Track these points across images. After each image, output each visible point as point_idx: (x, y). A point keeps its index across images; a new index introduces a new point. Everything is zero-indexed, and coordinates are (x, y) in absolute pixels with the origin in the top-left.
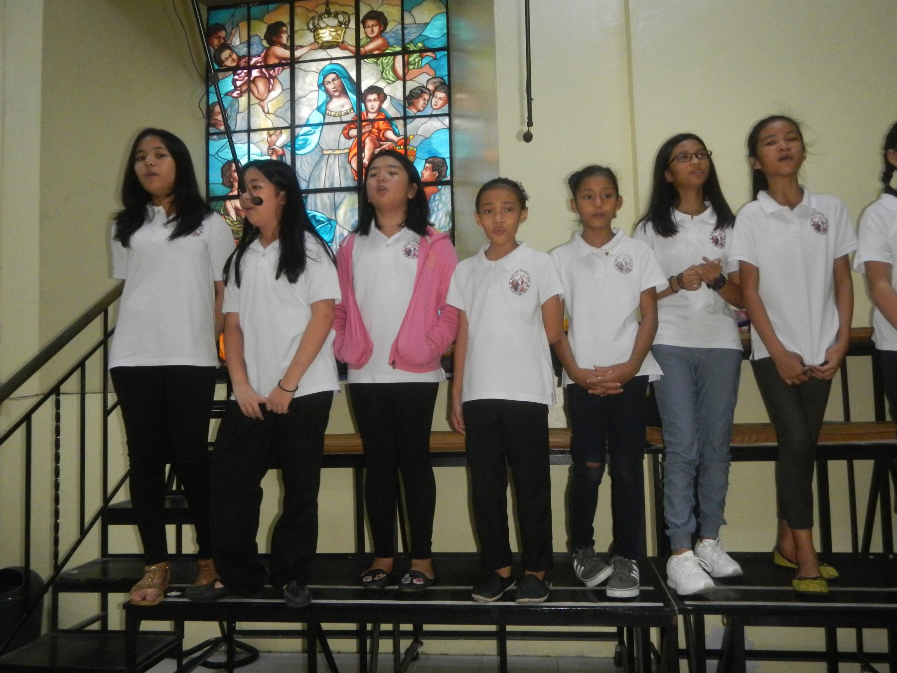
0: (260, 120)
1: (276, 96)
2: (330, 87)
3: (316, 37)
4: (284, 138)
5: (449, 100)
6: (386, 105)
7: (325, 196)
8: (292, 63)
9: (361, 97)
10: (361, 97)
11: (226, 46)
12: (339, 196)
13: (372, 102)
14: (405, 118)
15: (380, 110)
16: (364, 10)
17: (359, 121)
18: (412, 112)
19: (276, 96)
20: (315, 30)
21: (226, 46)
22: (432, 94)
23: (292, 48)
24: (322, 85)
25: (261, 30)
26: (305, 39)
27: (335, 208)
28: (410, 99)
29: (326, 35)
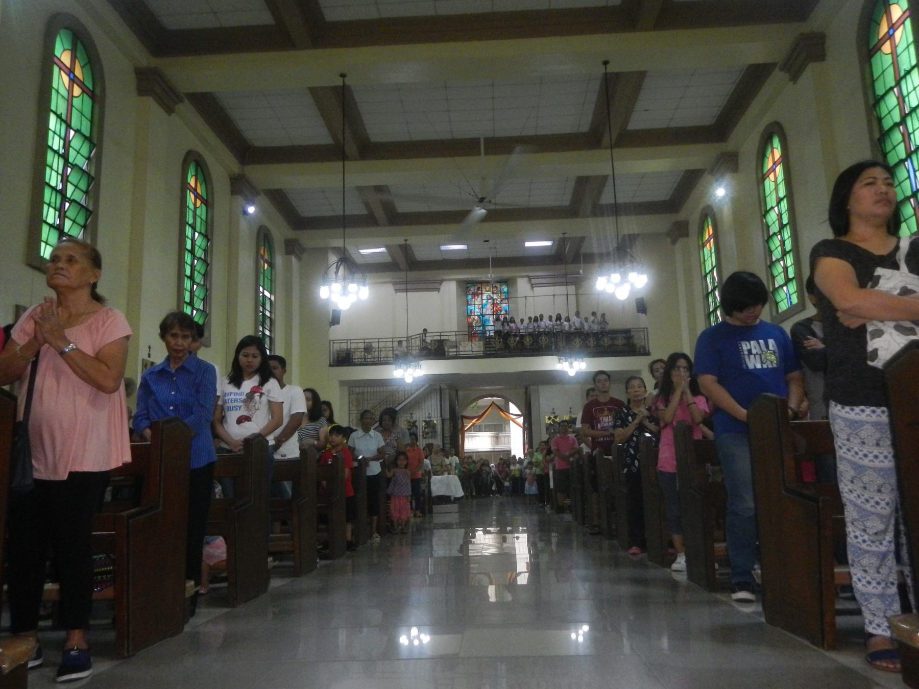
0: (476, 303)
1: (479, 299)
4: (481, 306)
5: (508, 301)
8: (482, 294)
10: (494, 300)
11: (470, 290)
14: (501, 304)
16: (494, 286)
19: (479, 299)
20: (486, 288)
21: (470, 290)
23: (482, 291)
24: (487, 298)
25: (476, 288)
26: (484, 290)
27: (490, 318)
28: (501, 301)
29: (487, 290)
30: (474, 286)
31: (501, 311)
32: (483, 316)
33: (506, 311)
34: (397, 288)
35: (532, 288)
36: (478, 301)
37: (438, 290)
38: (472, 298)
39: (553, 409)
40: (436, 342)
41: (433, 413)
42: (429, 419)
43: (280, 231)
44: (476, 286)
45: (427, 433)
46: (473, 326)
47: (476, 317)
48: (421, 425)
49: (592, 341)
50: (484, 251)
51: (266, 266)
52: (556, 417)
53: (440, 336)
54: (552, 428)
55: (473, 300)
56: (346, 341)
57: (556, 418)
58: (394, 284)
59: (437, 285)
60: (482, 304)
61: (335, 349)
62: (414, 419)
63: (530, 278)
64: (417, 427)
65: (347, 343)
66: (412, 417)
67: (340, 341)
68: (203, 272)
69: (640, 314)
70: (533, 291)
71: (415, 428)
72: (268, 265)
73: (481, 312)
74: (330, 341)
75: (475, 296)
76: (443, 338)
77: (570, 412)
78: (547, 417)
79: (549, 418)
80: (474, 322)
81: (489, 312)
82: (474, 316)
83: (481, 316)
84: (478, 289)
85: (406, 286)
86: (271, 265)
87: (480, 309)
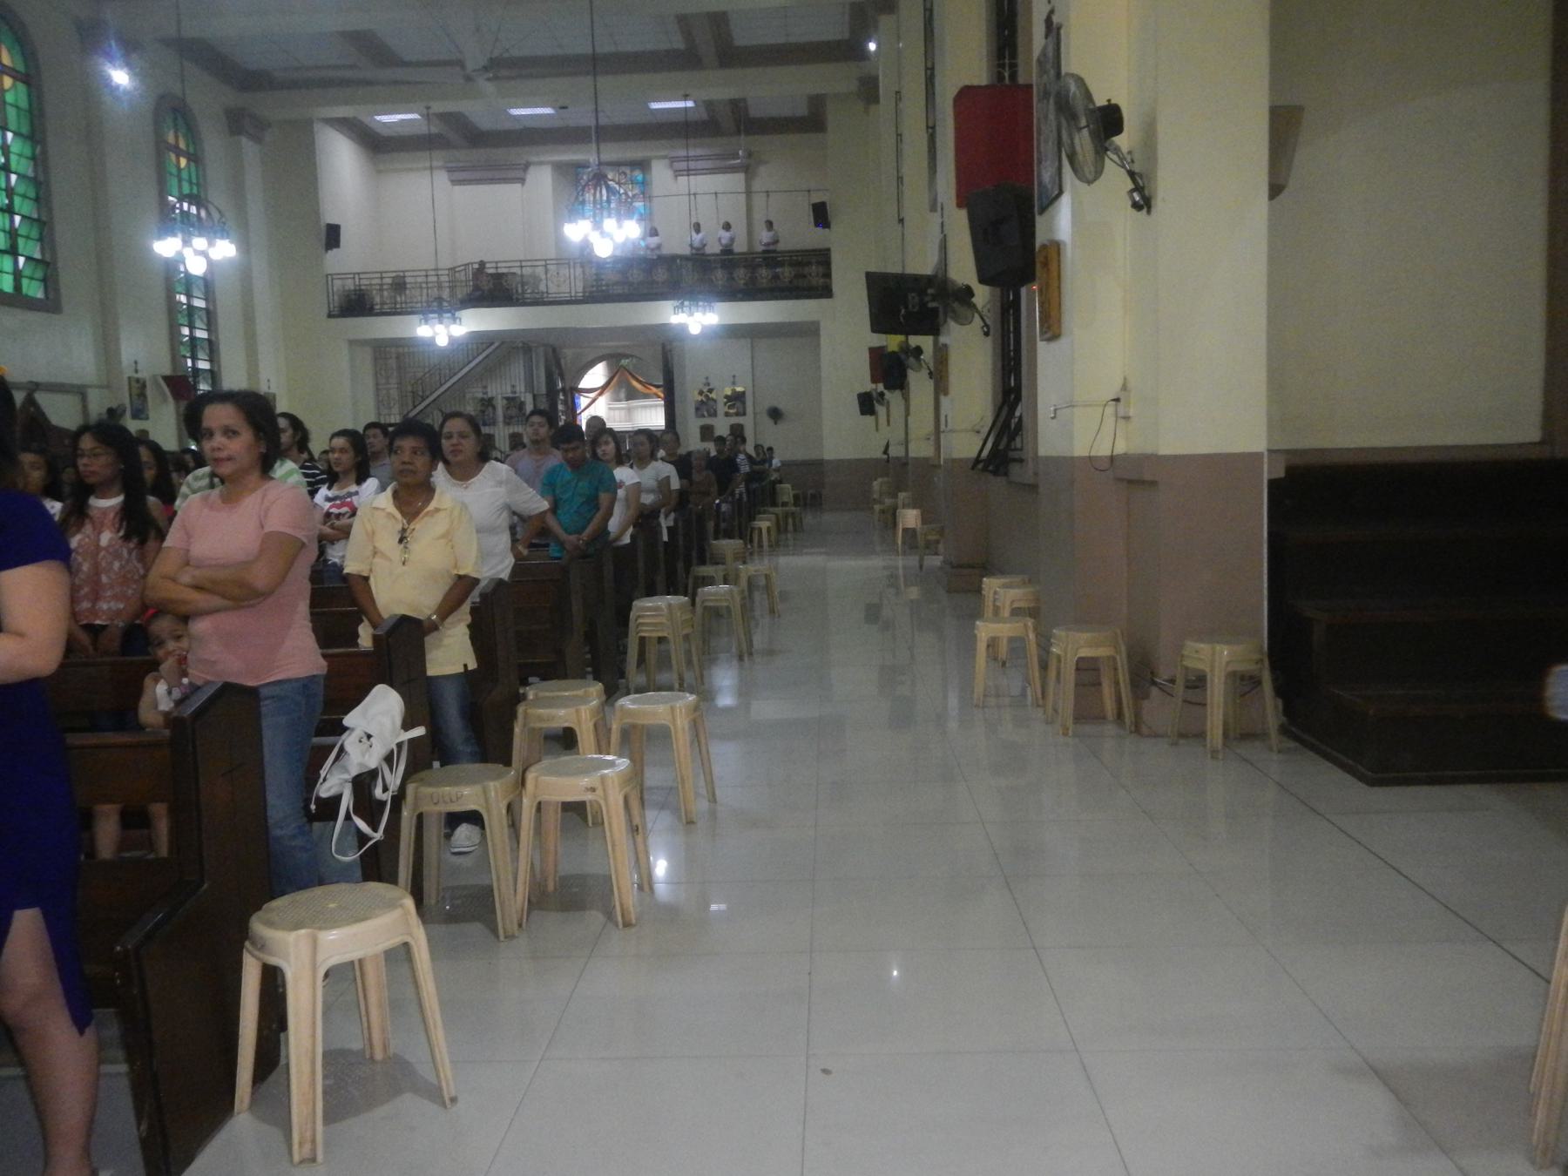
34: (453, 178)
35: (676, 176)
37: (522, 181)
39: (707, 378)
40: (489, 278)
41: (518, 384)
42: (514, 395)
43: (208, 99)
45: (511, 417)
48: (500, 404)
49: (741, 274)
50: (581, 116)
51: (183, 162)
52: (711, 391)
53: (497, 268)
56: (352, 276)
57: (711, 393)
58: (448, 171)
59: (519, 174)
61: (335, 289)
62: (490, 395)
63: (673, 160)
64: (494, 408)
65: (354, 278)
66: (486, 393)
67: (342, 276)
68: (32, 194)
69: (819, 229)
70: (676, 179)
71: (490, 409)
72: (189, 160)
74: (327, 276)
76: (500, 271)
78: (696, 393)
79: (701, 393)
85: (464, 175)
86: (195, 159)
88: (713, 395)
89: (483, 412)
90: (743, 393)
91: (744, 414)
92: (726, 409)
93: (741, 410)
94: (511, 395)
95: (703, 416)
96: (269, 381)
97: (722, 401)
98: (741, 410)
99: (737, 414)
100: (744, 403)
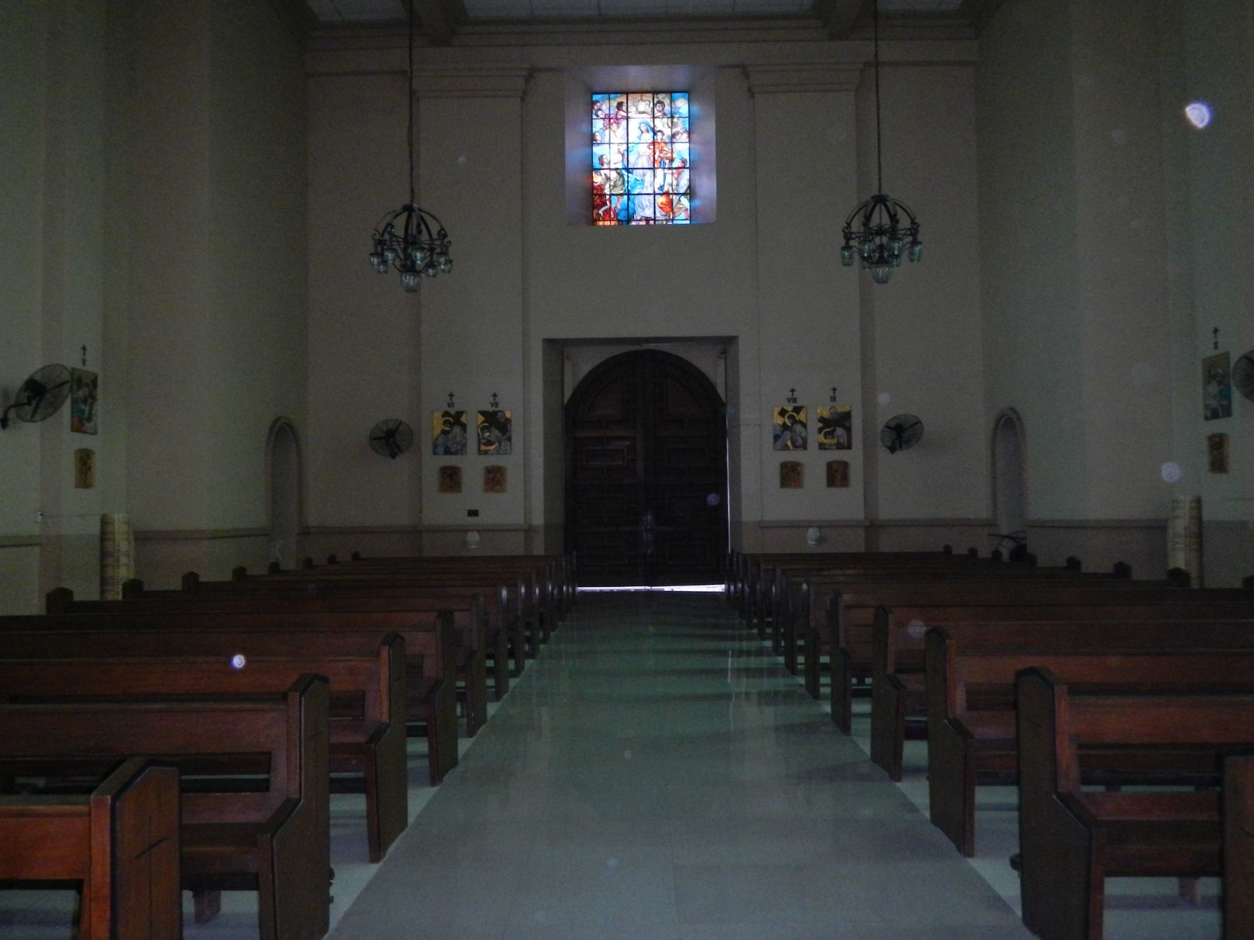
2: (643, 129)
3: (637, 109)
4: (624, 147)
5: (689, 137)
6: (664, 137)
7: (641, 171)
9: (655, 134)
12: (646, 171)
13: (659, 136)
15: (662, 139)
17: (654, 143)
18: (674, 140)
22: (682, 134)
23: (627, 112)
25: (614, 104)
26: (632, 109)
27: (644, 175)
30: (609, 99)
31: (672, 160)
32: (628, 170)
33: (684, 161)
36: (618, 133)
38: (605, 128)
42: (494, 409)
44: (614, 99)
46: (605, 195)
47: (614, 175)
48: (474, 421)
52: (798, 410)
54: (788, 434)
55: (607, 131)
57: (798, 413)
60: (628, 143)
62: (457, 408)
64: (464, 427)
71: (457, 429)
73: (626, 164)
75: (610, 124)
77: (833, 399)
78: (777, 410)
79: (783, 412)
80: (607, 186)
81: (644, 162)
82: (607, 172)
83: (624, 172)
84: (620, 106)
87: (623, 155)
88: (802, 416)
89: (444, 433)
90: (847, 416)
91: (849, 447)
92: (821, 438)
93: (844, 440)
94: (490, 409)
95: (786, 447)
96: (84, 349)
97: (814, 426)
98: (844, 440)
99: (839, 446)
100: (849, 430)
